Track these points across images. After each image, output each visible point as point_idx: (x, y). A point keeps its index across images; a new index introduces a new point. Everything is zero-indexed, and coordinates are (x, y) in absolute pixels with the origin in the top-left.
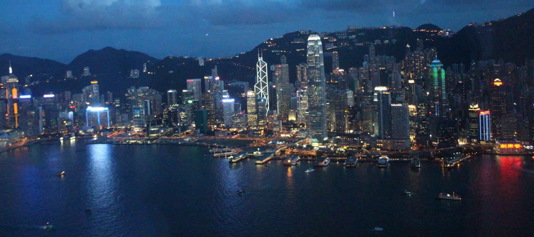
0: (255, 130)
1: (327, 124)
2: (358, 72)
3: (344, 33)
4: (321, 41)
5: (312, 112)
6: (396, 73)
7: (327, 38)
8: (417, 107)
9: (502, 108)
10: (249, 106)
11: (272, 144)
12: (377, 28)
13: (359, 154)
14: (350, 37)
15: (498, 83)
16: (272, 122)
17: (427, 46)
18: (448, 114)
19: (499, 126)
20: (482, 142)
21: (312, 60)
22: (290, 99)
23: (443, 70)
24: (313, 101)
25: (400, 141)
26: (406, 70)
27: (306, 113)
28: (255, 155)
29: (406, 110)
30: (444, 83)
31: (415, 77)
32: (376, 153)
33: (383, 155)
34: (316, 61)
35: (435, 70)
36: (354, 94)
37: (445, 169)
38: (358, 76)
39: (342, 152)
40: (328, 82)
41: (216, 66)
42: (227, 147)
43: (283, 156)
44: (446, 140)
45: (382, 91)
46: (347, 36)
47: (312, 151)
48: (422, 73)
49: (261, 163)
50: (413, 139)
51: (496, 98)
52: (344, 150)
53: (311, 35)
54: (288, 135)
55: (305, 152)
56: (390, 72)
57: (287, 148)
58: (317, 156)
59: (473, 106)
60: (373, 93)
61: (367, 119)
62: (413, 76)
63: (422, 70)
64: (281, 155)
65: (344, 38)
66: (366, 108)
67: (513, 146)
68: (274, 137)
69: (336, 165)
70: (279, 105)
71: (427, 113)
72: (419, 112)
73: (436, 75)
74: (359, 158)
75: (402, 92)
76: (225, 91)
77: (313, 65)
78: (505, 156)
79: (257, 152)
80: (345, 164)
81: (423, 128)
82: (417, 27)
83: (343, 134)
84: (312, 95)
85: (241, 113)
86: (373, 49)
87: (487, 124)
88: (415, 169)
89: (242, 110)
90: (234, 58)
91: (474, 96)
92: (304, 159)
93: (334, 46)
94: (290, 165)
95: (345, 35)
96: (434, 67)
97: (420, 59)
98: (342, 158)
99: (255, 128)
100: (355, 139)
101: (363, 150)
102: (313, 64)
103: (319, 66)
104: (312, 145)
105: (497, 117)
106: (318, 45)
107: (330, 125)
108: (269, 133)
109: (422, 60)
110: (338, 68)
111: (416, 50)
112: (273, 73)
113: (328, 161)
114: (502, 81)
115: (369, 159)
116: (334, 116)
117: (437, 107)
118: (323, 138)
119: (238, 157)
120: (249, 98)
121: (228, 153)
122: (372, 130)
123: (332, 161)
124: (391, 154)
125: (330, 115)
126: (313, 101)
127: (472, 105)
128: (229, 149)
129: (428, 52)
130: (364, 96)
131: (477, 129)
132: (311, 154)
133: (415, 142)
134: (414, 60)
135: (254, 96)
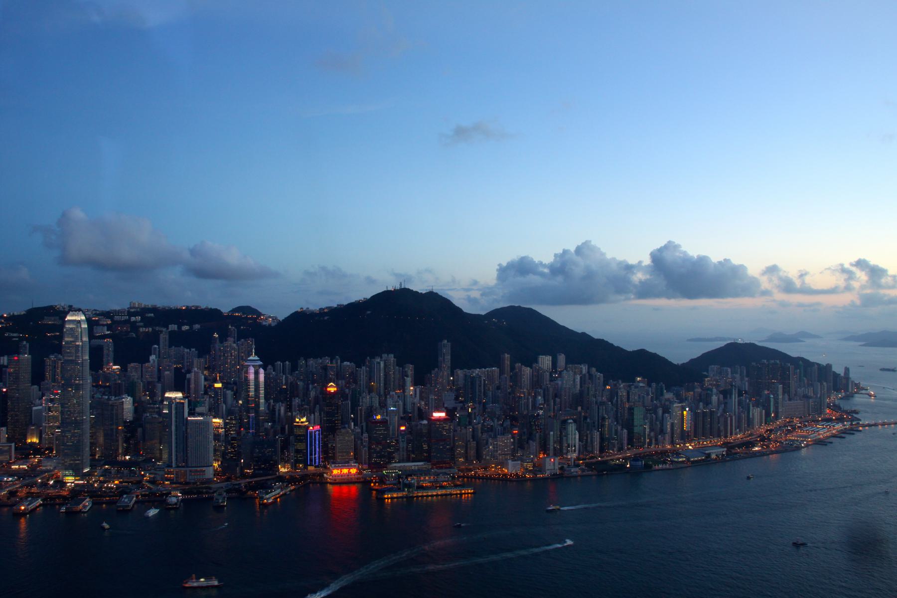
1: (91, 447)
4: (86, 323)
8: (224, 421)
12: (173, 308)
13: (138, 491)
14: (133, 319)
17: (241, 336)
18: (266, 429)
19: (332, 446)
20: (309, 468)
21: (70, 350)
23: (262, 371)
24: (69, 413)
29: (207, 424)
30: (262, 387)
32: (165, 488)
35: (252, 370)
36: (134, 402)
37: (261, 506)
39: (112, 488)
45: (176, 398)
46: (127, 317)
51: (331, 409)
55: (51, 492)
56: (189, 371)
58: (72, 498)
59: (300, 420)
60: (162, 401)
65: (123, 319)
67: (349, 471)
72: (227, 428)
73: (252, 377)
75: (205, 400)
78: (338, 485)
83: (113, 462)
84: (67, 404)
86: (165, 337)
87: (317, 443)
88: (219, 508)
91: (302, 405)
93: (108, 330)
95: (124, 316)
96: (249, 366)
97: (231, 354)
102: (72, 356)
104: (63, 480)
111: (226, 340)
112: (4, 369)
114: (337, 386)
117: (253, 421)
118: (83, 469)
123: (94, 504)
124: (185, 489)
126: (69, 413)
127: (298, 418)
129: (242, 345)
130: (149, 406)
131: (304, 450)
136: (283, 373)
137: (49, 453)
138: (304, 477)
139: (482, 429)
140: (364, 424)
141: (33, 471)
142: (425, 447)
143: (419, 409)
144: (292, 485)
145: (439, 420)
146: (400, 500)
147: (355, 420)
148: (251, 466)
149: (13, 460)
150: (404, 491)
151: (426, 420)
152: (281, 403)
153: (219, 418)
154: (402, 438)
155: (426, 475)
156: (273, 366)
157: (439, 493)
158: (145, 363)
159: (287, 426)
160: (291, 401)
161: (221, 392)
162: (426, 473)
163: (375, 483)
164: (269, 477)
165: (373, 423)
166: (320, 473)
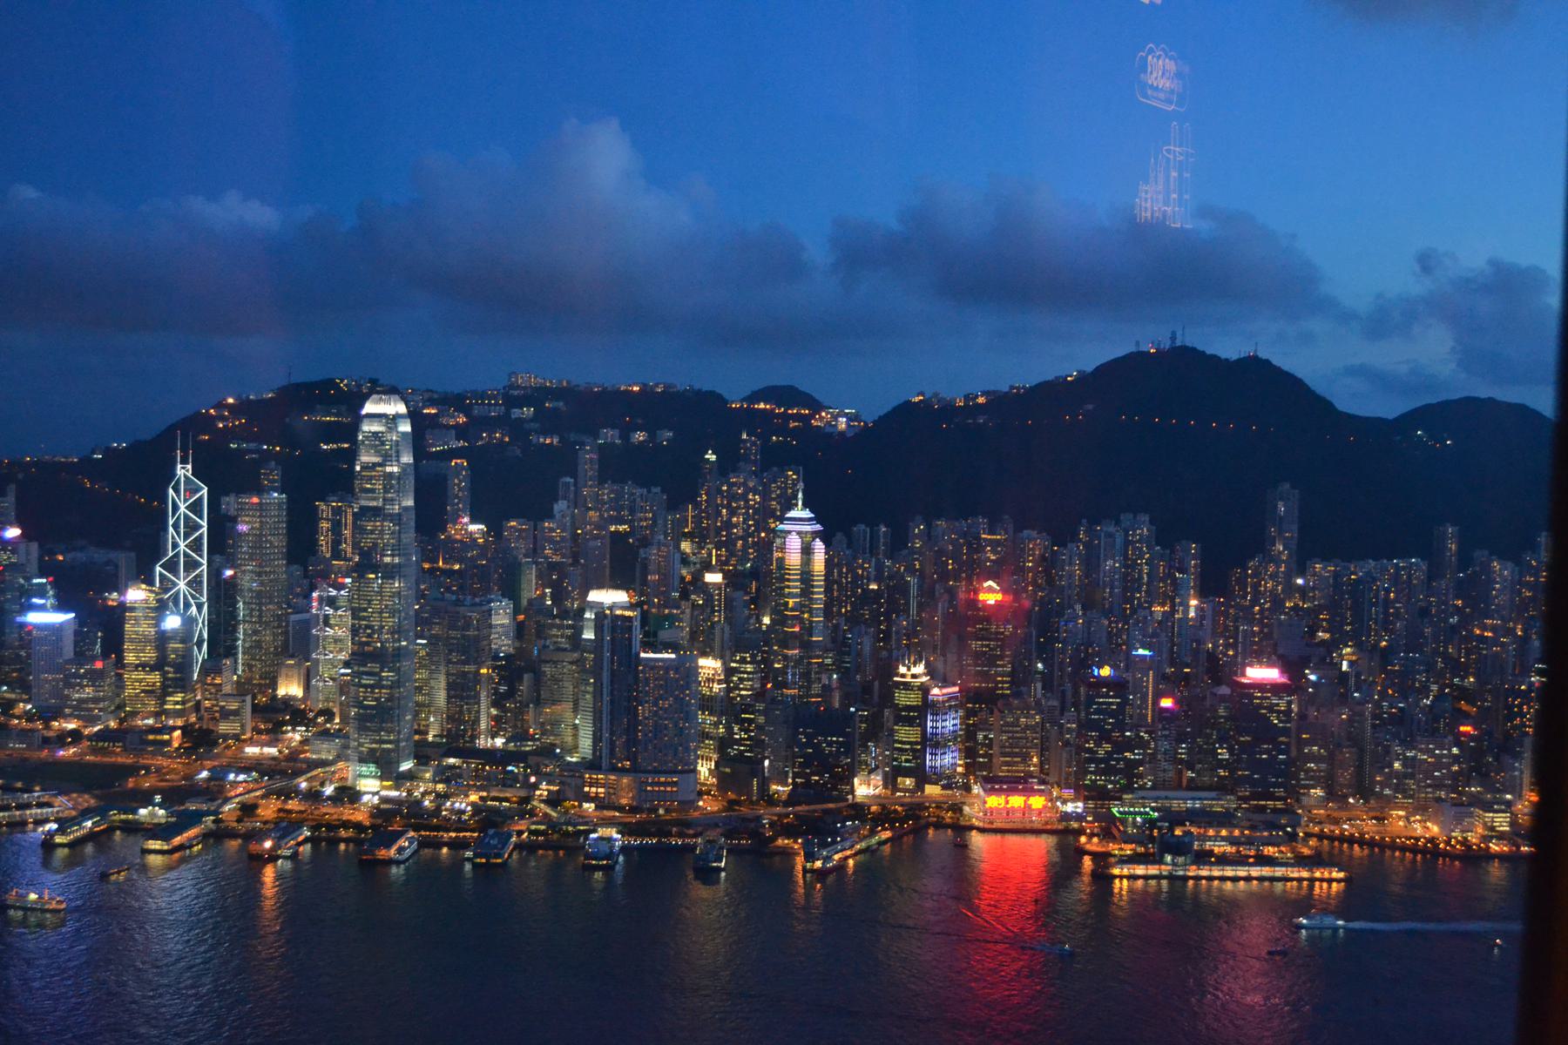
0: (152, 730)
1: (416, 714)
2: (535, 537)
3: (495, 397)
5: (361, 669)
6: (665, 545)
7: (433, 411)
8: (724, 664)
9: (999, 679)
10: (132, 641)
11: (209, 780)
12: (609, 389)
14: (516, 413)
15: (991, 594)
16: (217, 700)
18: (827, 689)
19: (986, 737)
22: (288, 622)
23: (819, 546)
24: (369, 631)
25: (663, 779)
26: (699, 537)
27: (343, 671)
28: (143, 819)
31: (727, 563)
32: (583, 817)
33: (602, 826)
34: (386, 491)
35: (794, 543)
36: (516, 611)
37: (808, 875)
38: (535, 552)
39: (464, 812)
40: (426, 566)
41: (13, 487)
42: (37, 788)
43: (248, 825)
44: (817, 778)
47: (354, 809)
48: (751, 551)
49: (166, 847)
50: (707, 775)
51: (982, 646)
52: (469, 808)
53: (375, 396)
54: (273, 751)
55: (329, 811)
56: (645, 542)
57: (263, 797)
59: (909, 669)
60: (581, 611)
61: (555, 702)
62: (720, 561)
63: (753, 541)
64: (239, 821)
66: (555, 662)
67: (1025, 801)
68: (218, 756)
69: (436, 859)
70: (244, 640)
71: (757, 685)
72: (732, 682)
73: (794, 558)
74: (520, 833)
75: (683, 613)
76: (44, 581)
77: (375, 504)
78: (999, 836)
79: (150, 808)
80: (469, 854)
81: (744, 735)
82: (747, 392)
84: (365, 610)
85: (99, 665)
86: (591, 459)
88: (707, 875)
89: (105, 655)
90: (86, 461)
91: (916, 634)
92: (324, 835)
94: (273, 858)
97: (747, 501)
98: (461, 834)
99: (150, 721)
100: (510, 768)
101: (534, 808)
103: (397, 507)
105: (980, 708)
106: (398, 432)
107: (427, 719)
108: (200, 740)
109: (753, 507)
110: (466, 520)
111: (735, 470)
112: (229, 525)
113: (411, 843)
114: (1004, 591)
115: (556, 836)
116: (443, 684)
118: (398, 764)
119: (79, 824)
120: (132, 609)
121: (39, 811)
122: (569, 739)
123: (424, 844)
124: (630, 823)
125: (426, 682)
126: (369, 631)
127: (904, 665)
128: (43, 796)
129: (775, 482)
131: (917, 743)
132: (352, 818)
133: (712, 785)
134: (728, 507)
135: (154, 604)
136: (871, 552)
137: (327, 721)
138: (915, 810)
139: (1375, 716)
140: (1068, 686)
141: (292, 765)
142: (1223, 754)
143: (1212, 657)
144: (886, 829)
145: (1260, 686)
146: (1153, 882)
147: (1047, 680)
148: (787, 777)
149: (248, 735)
150: (1161, 862)
151: (1228, 685)
152: (863, 626)
153: (715, 658)
154: (1164, 729)
155: (1222, 825)
156: (849, 535)
157: (1254, 874)
158: (543, 520)
159: (876, 683)
160: (888, 620)
161: (720, 595)
162: (1225, 819)
163: (1092, 835)
164: (831, 806)
165: (1090, 685)
166: (956, 804)
